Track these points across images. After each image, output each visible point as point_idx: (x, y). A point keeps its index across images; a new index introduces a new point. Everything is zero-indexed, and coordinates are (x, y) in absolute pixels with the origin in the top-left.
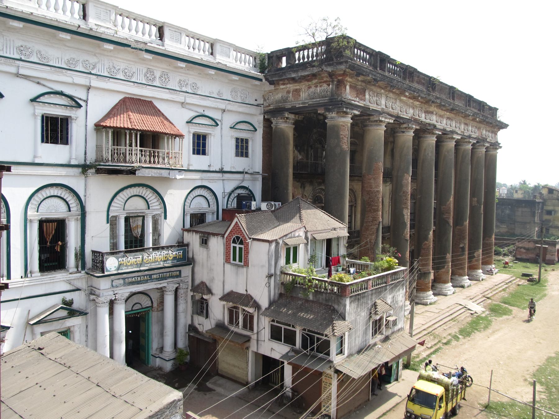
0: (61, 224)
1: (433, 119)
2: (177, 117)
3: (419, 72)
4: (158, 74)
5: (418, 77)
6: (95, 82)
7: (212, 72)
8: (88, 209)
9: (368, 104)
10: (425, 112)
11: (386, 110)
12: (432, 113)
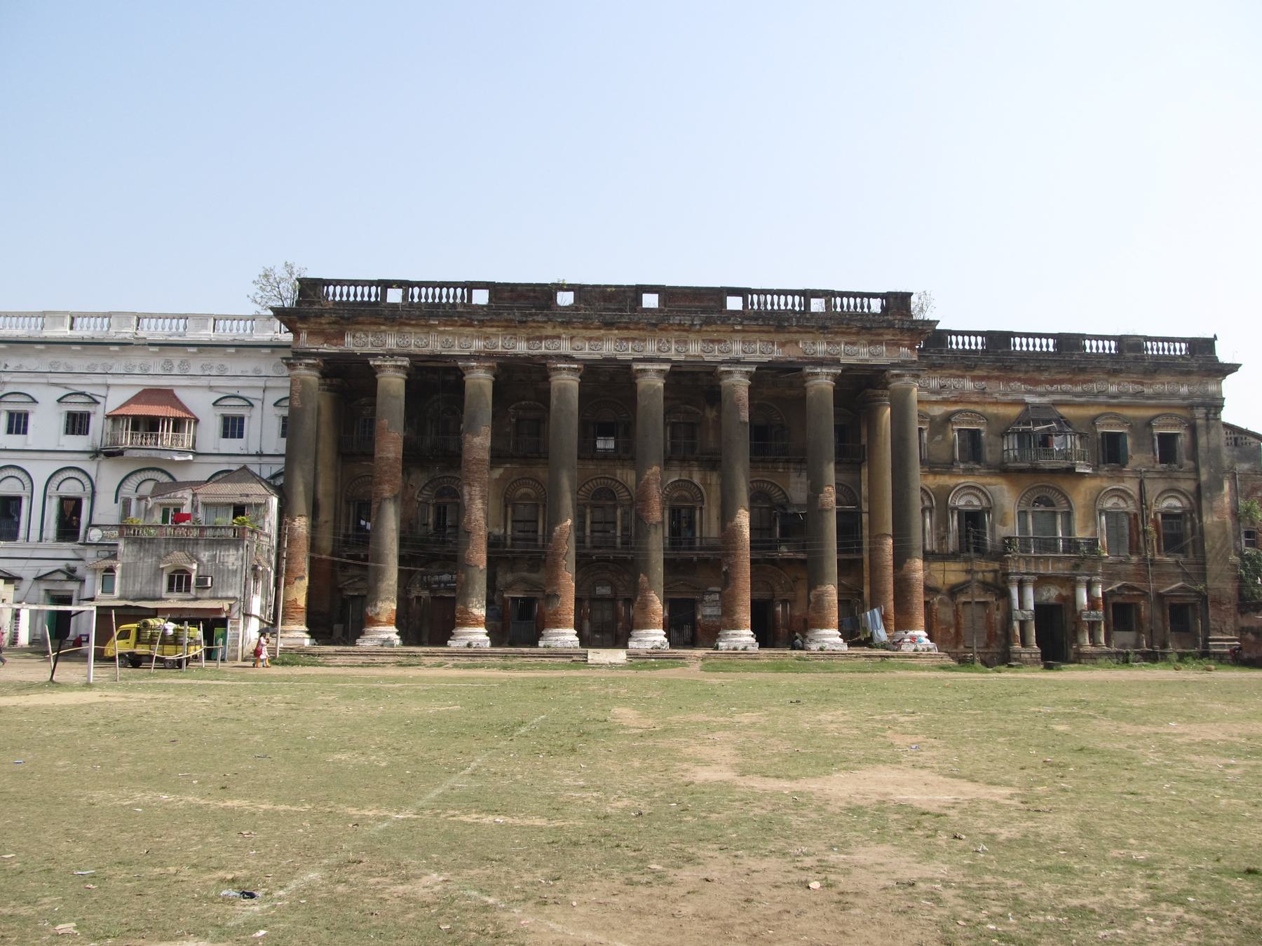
0: (78, 502)
1: (565, 347)
2: (199, 401)
4: (176, 363)
5: (512, 291)
6: (110, 380)
7: (232, 350)
8: (98, 489)
9: (352, 347)
10: (528, 340)
11: (398, 350)
12: (559, 337)
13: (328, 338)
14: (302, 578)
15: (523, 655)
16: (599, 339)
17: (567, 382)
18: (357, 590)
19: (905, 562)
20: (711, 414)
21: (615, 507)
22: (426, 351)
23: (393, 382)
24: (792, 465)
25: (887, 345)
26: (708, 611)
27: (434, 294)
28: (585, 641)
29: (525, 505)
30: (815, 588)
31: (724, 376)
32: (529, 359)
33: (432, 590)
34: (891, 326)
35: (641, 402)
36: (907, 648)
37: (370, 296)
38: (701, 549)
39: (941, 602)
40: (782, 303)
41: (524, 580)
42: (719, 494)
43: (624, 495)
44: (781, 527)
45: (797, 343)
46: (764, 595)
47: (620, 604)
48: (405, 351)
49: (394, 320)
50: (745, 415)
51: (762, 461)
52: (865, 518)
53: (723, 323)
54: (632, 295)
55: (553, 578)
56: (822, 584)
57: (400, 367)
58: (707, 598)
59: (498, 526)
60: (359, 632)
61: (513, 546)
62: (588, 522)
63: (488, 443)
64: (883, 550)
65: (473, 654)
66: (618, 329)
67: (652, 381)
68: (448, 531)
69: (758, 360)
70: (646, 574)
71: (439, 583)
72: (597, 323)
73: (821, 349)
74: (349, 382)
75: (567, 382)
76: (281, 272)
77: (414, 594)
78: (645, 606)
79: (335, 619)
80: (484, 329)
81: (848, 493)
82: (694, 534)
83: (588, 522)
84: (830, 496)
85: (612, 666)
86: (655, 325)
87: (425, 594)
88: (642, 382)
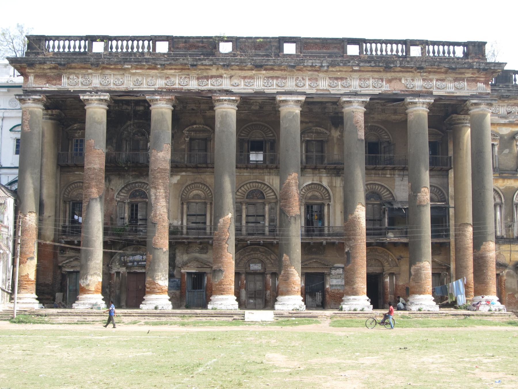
1: (226, 84)
3: (182, 38)
5: (185, 42)
10: (198, 79)
12: (221, 77)
13: (49, 80)
14: (32, 258)
15: (197, 315)
16: (251, 77)
17: (227, 111)
18: (72, 267)
19: (482, 244)
20: (335, 134)
21: (264, 204)
22: (123, 88)
23: (97, 112)
24: (397, 172)
25: (468, 81)
26: (334, 282)
27: (127, 45)
28: (242, 305)
29: (197, 203)
30: (414, 264)
31: (346, 105)
32: (199, 93)
33: (128, 267)
34: (471, 67)
35: (284, 124)
36: (484, 309)
37: (80, 48)
38: (329, 235)
39: (508, 274)
40: (389, 50)
41: (197, 260)
42: (342, 194)
43: (270, 195)
44: (389, 219)
45: (400, 80)
46: (376, 269)
47: (268, 277)
48: (106, 88)
49: (97, 65)
50: (361, 134)
51: (374, 169)
52: (452, 211)
53: (345, 65)
54: (276, 44)
55: (218, 258)
56: (420, 261)
57: (102, 100)
58: (333, 272)
59: (176, 219)
60: (75, 299)
61: (187, 233)
62: (244, 216)
63: (169, 157)
64: (465, 236)
65: (158, 314)
66: (266, 70)
67: (291, 110)
68: (140, 223)
69: (371, 92)
70: (288, 254)
71: (133, 262)
72: (249, 65)
73: (418, 84)
74: (66, 112)
75: (227, 111)
76: (14, 32)
77: (113, 271)
78: (287, 278)
79: (57, 288)
80: (165, 71)
81: (439, 193)
82: (323, 224)
83: (244, 216)
84: (425, 195)
85: (263, 323)
86: (294, 67)
87: (123, 270)
88: (284, 110)
